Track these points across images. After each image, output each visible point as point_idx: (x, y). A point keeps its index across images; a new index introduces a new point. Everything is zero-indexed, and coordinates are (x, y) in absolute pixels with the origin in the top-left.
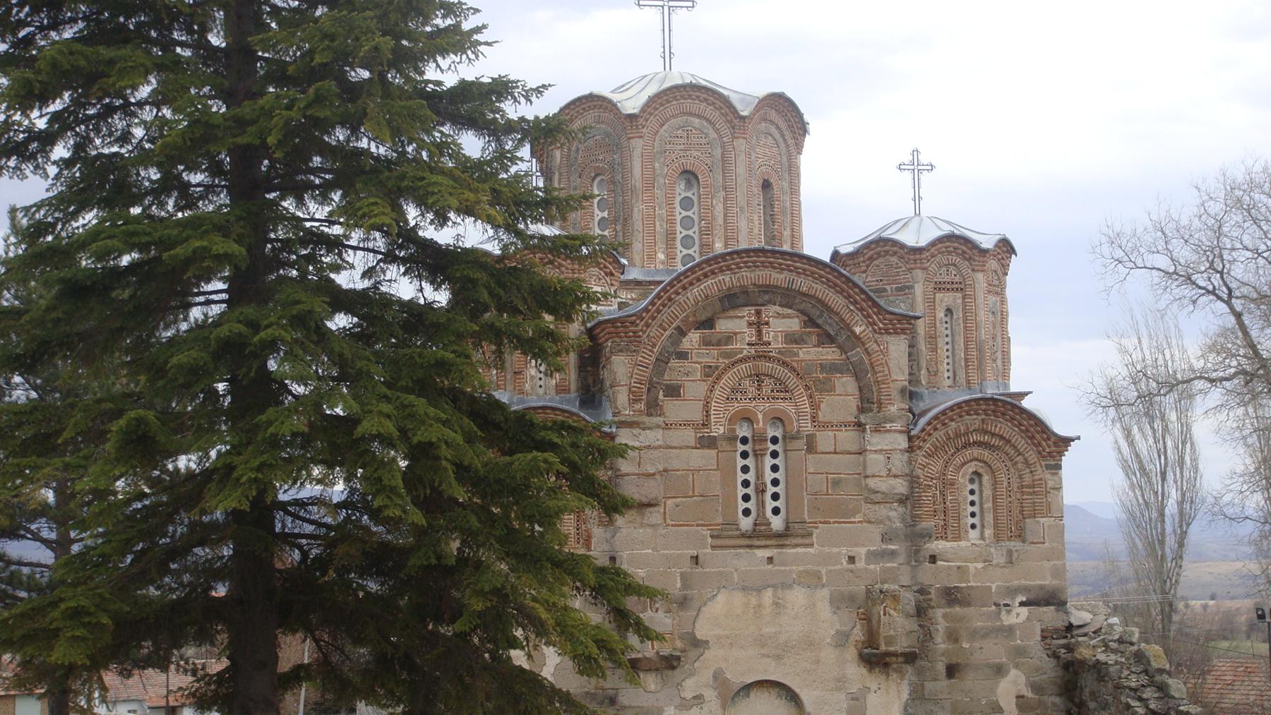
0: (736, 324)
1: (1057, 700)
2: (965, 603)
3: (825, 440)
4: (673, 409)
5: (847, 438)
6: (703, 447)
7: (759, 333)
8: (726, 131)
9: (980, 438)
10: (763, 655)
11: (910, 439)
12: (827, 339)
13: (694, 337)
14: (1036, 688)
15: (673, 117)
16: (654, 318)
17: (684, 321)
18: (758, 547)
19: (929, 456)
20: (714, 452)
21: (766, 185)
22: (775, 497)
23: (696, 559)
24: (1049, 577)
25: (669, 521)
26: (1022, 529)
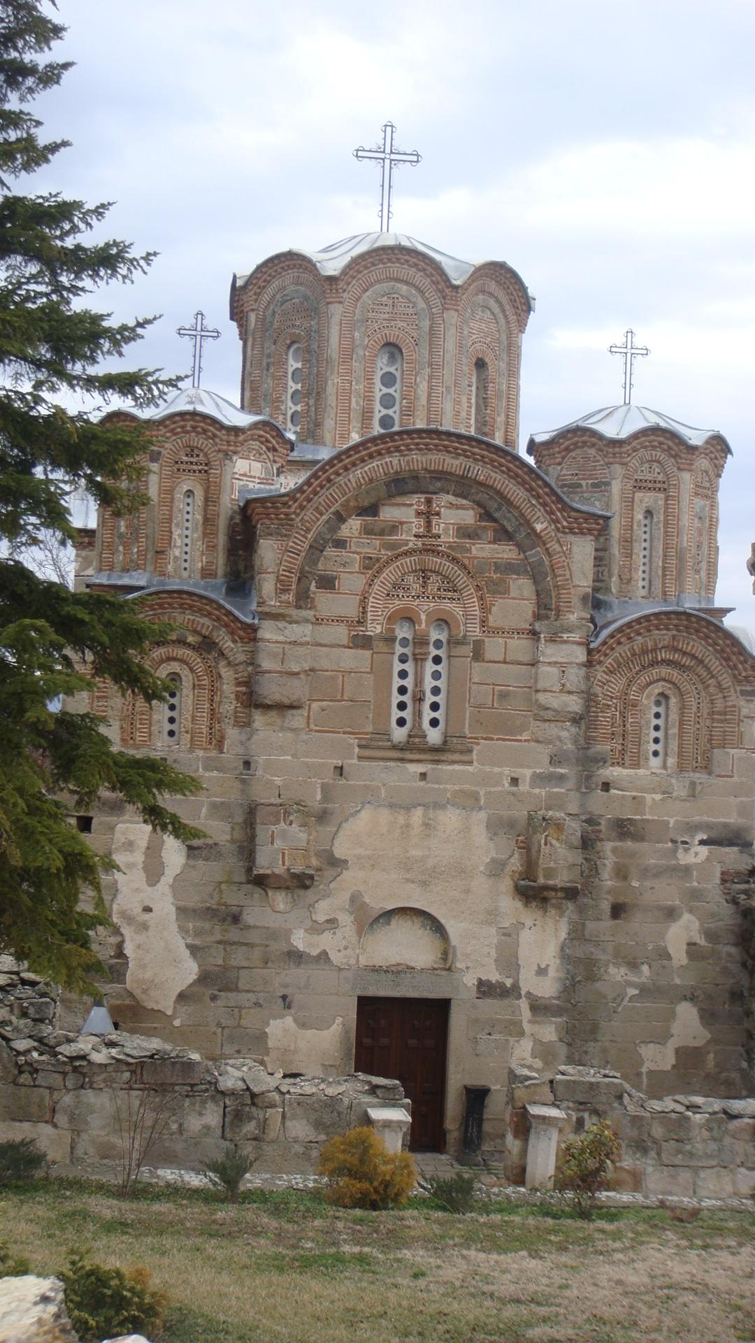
0: (403, 513)
1: (733, 950)
2: (638, 837)
3: (494, 648)
4: (326, 603)
5: (519, 647)
6: (356, 646)
7: (429, 525)
8: (436, 301)
9: (669, 656)
10: (408, 880)
12: (504, 535)
14: (710, 935)
15: (379, 281)
16: (309, 500)
17: (345, 505)
18: (411, 761)
19: (610, 672)
20: (368, 653)
21: (480, 364)
22: (435, 707)
23: (340, 770)
24: (735, 814)
25: (312, 726)
26: (709, 760)
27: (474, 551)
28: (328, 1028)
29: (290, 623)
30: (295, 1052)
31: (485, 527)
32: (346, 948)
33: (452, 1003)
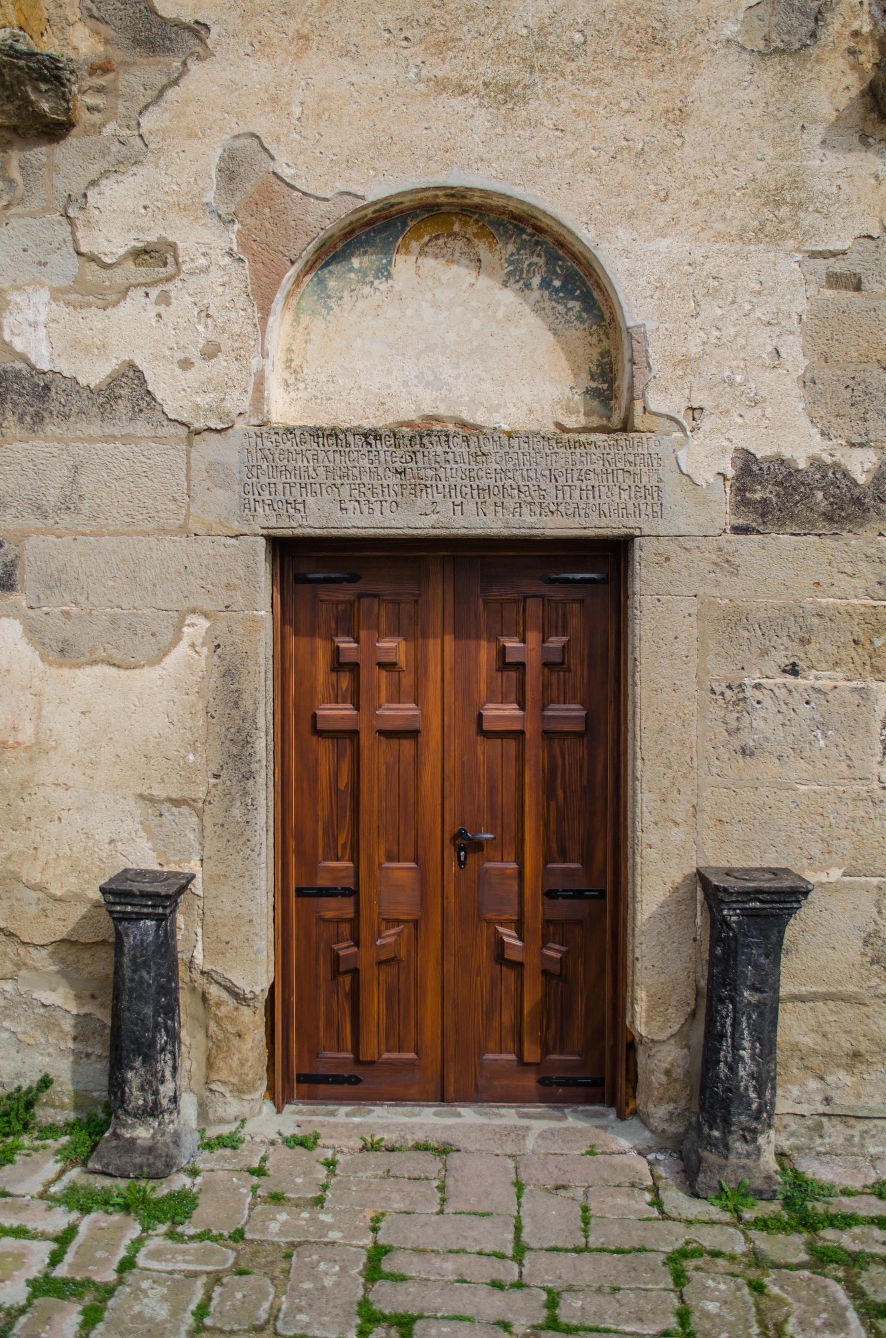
10: (441, 85)
28: (156, 660)
30: (38, 750)
32: (210, 352)
33: (643, 556)
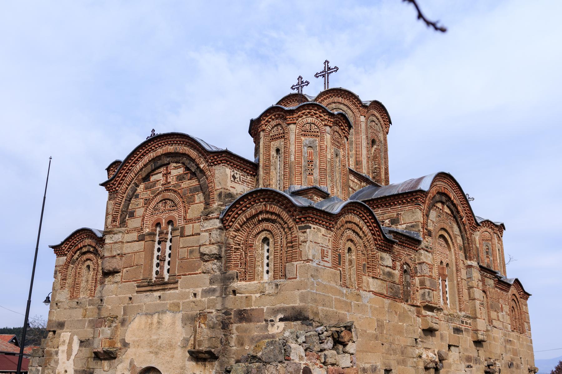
0: (158, 177)
3: (189, 229)
4: (133, 223)
9: (264, 216)
10: (151, 352)
11: (222, 221)
13: (142, 186)
16: (123, 180)
19: (237, 230)
20: (143, 242)
24: (298, 301)
27: (182, 186)
29: (114, 234)
31: (187, 173)
